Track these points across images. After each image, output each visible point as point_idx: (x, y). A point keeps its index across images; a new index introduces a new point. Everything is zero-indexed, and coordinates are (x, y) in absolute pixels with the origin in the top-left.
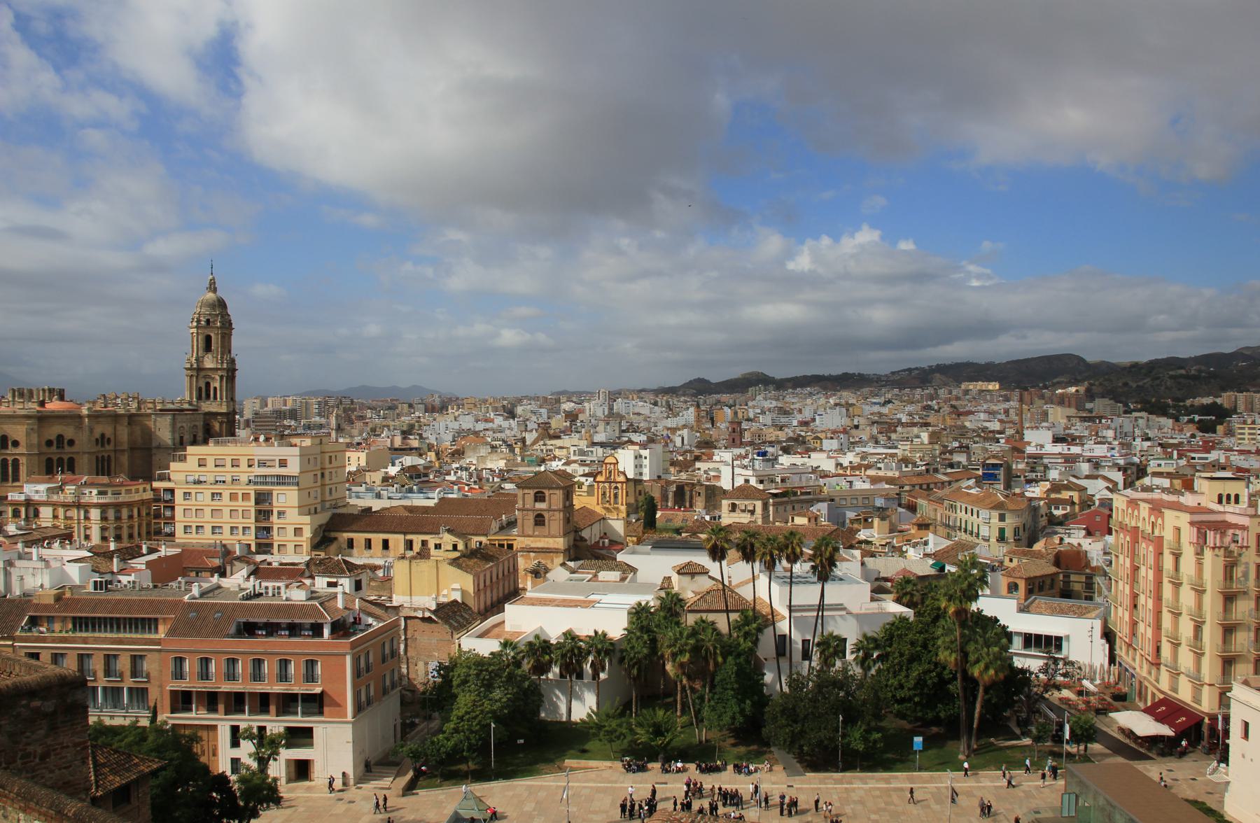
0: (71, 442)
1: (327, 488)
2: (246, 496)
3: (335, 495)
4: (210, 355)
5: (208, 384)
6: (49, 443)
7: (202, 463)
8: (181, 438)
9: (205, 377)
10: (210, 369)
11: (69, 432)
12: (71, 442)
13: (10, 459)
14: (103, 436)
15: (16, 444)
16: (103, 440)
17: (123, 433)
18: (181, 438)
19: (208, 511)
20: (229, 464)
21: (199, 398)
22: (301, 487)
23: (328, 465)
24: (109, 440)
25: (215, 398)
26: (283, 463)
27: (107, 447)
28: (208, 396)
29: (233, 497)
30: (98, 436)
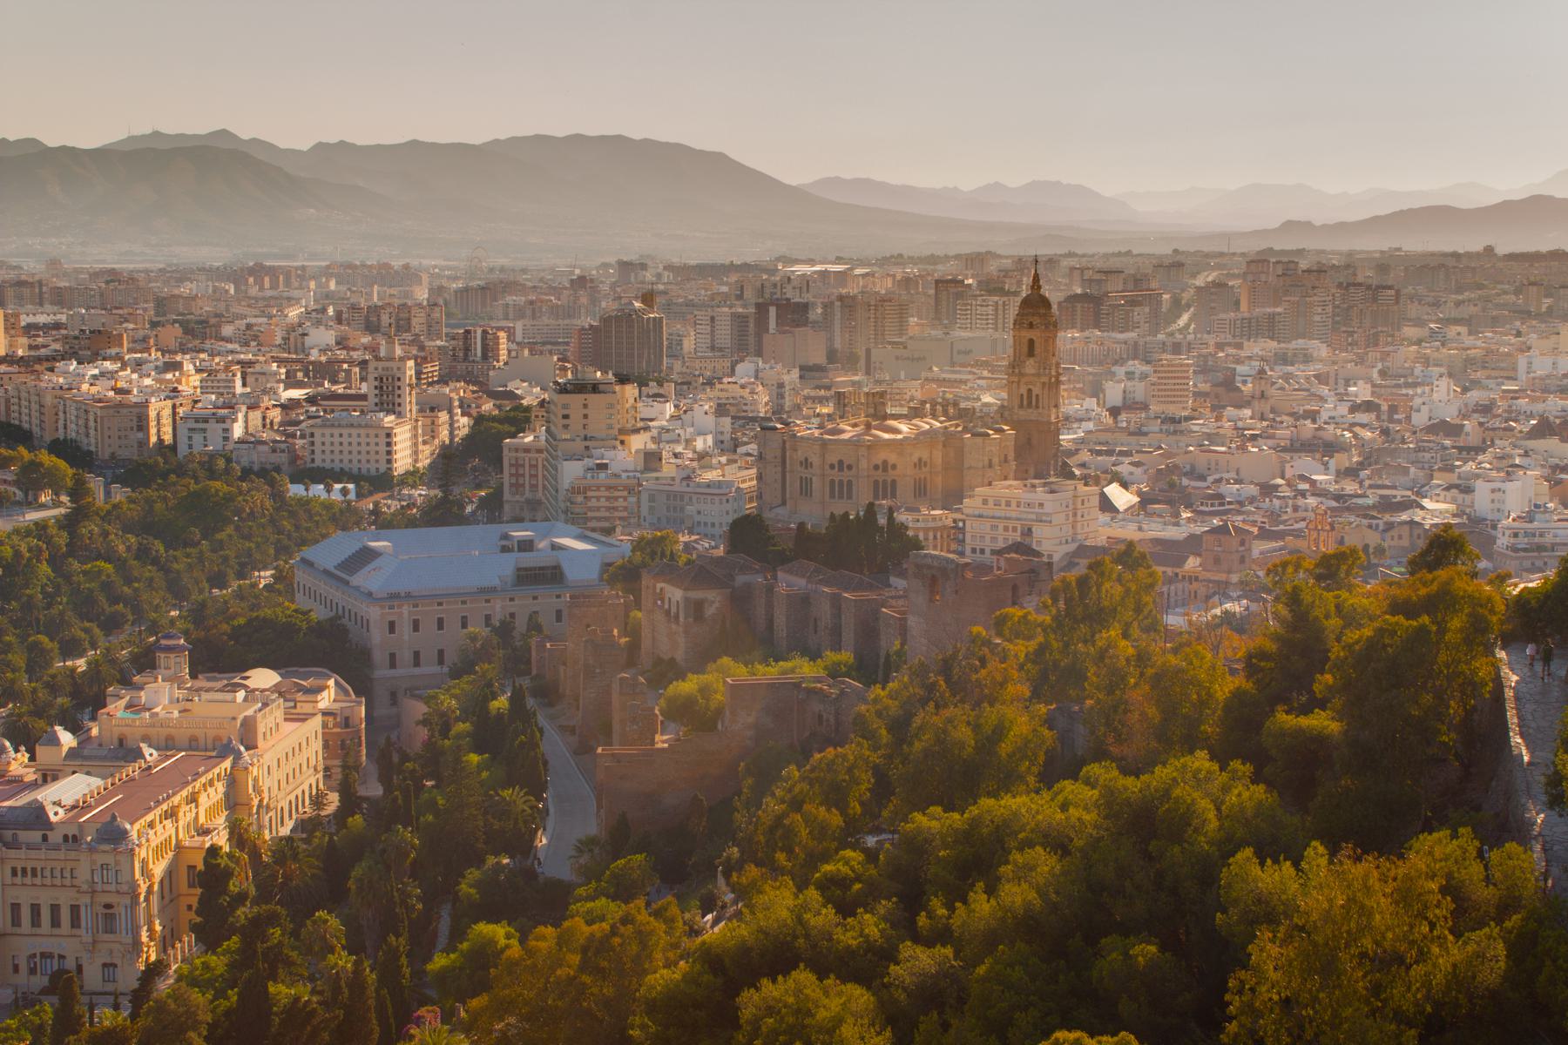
0: (894, 467)
1: (1079, 525)
2: (1015, 529)
3: (1086, 530)
4: (1031, 361)
5: (1030, 391)
6: (876, 467)
7: (985, 502)
8: (990, 461)
9: (1026, 384)
10: (1033, 375)
11: (892, 458)
12: (894, 467)
13: (845, 481)
14: (920, 460)
15: (850, 467)
16: (920, 463)
17: (938, 456)
18: (990, 461)
19: (988, 538)
20: (1003, 504)
21: (1021, 406)
22: (1054, 523)
23: (1079, 506)
24: (925, 465)
25: (1037, 407)
26: (1041, 505)
27: (924, 469)
28: (1030, 403)
29: (1006, 529)
30: (916, 460)
